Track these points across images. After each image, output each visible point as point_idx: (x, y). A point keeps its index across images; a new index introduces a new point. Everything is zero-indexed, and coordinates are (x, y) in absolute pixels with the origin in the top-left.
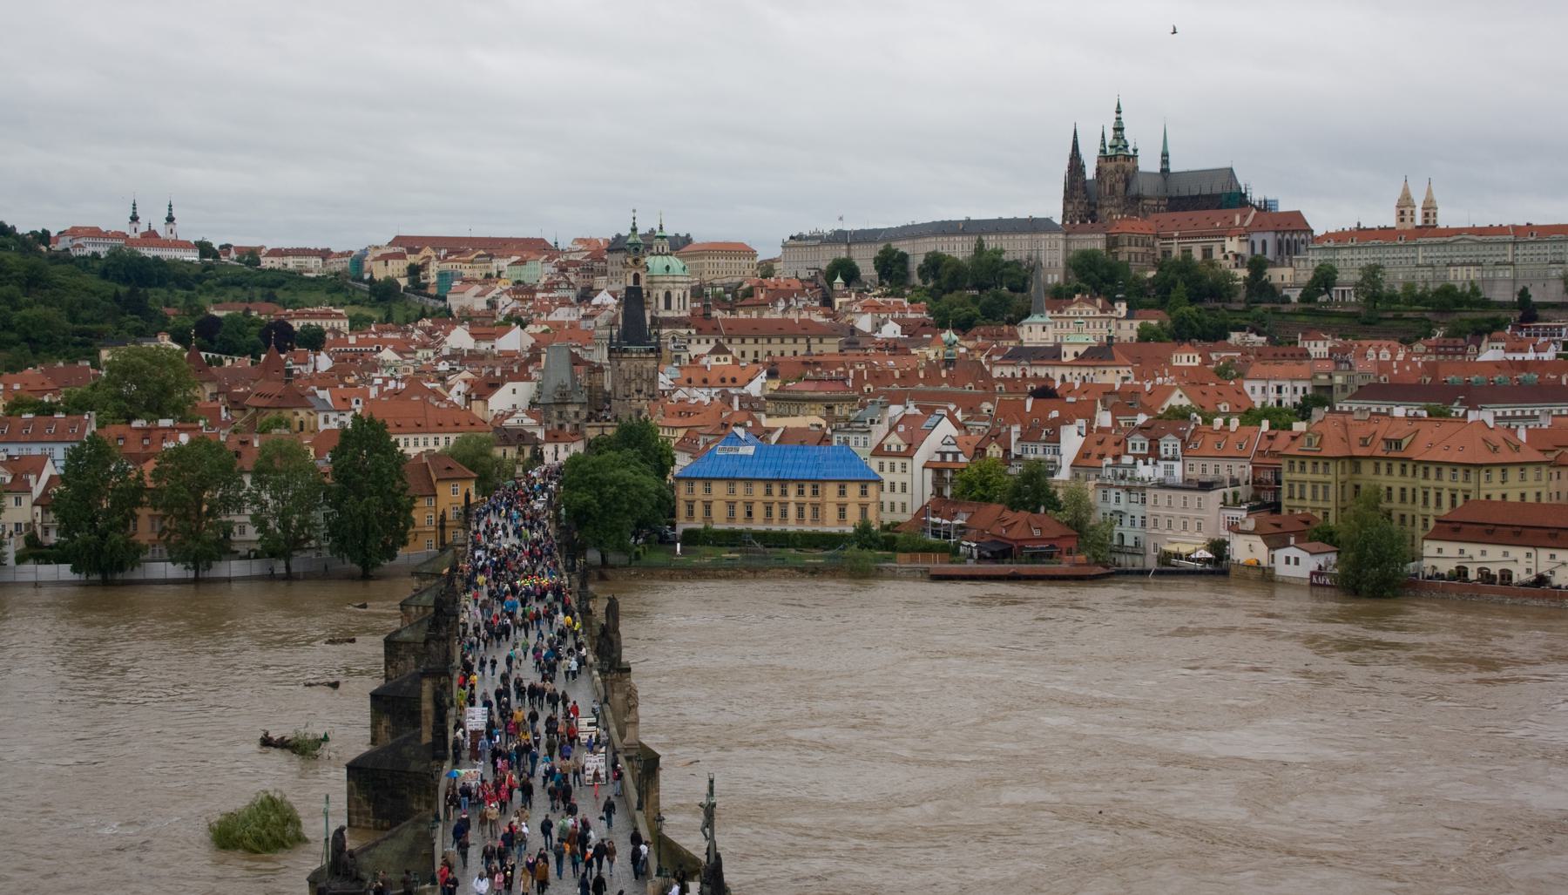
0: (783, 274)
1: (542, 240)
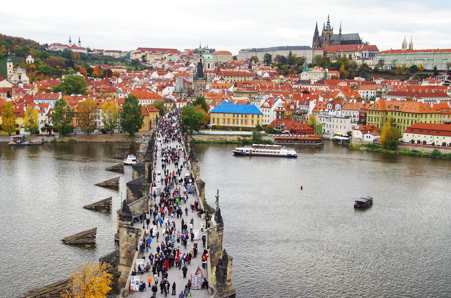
0: (239, 59)
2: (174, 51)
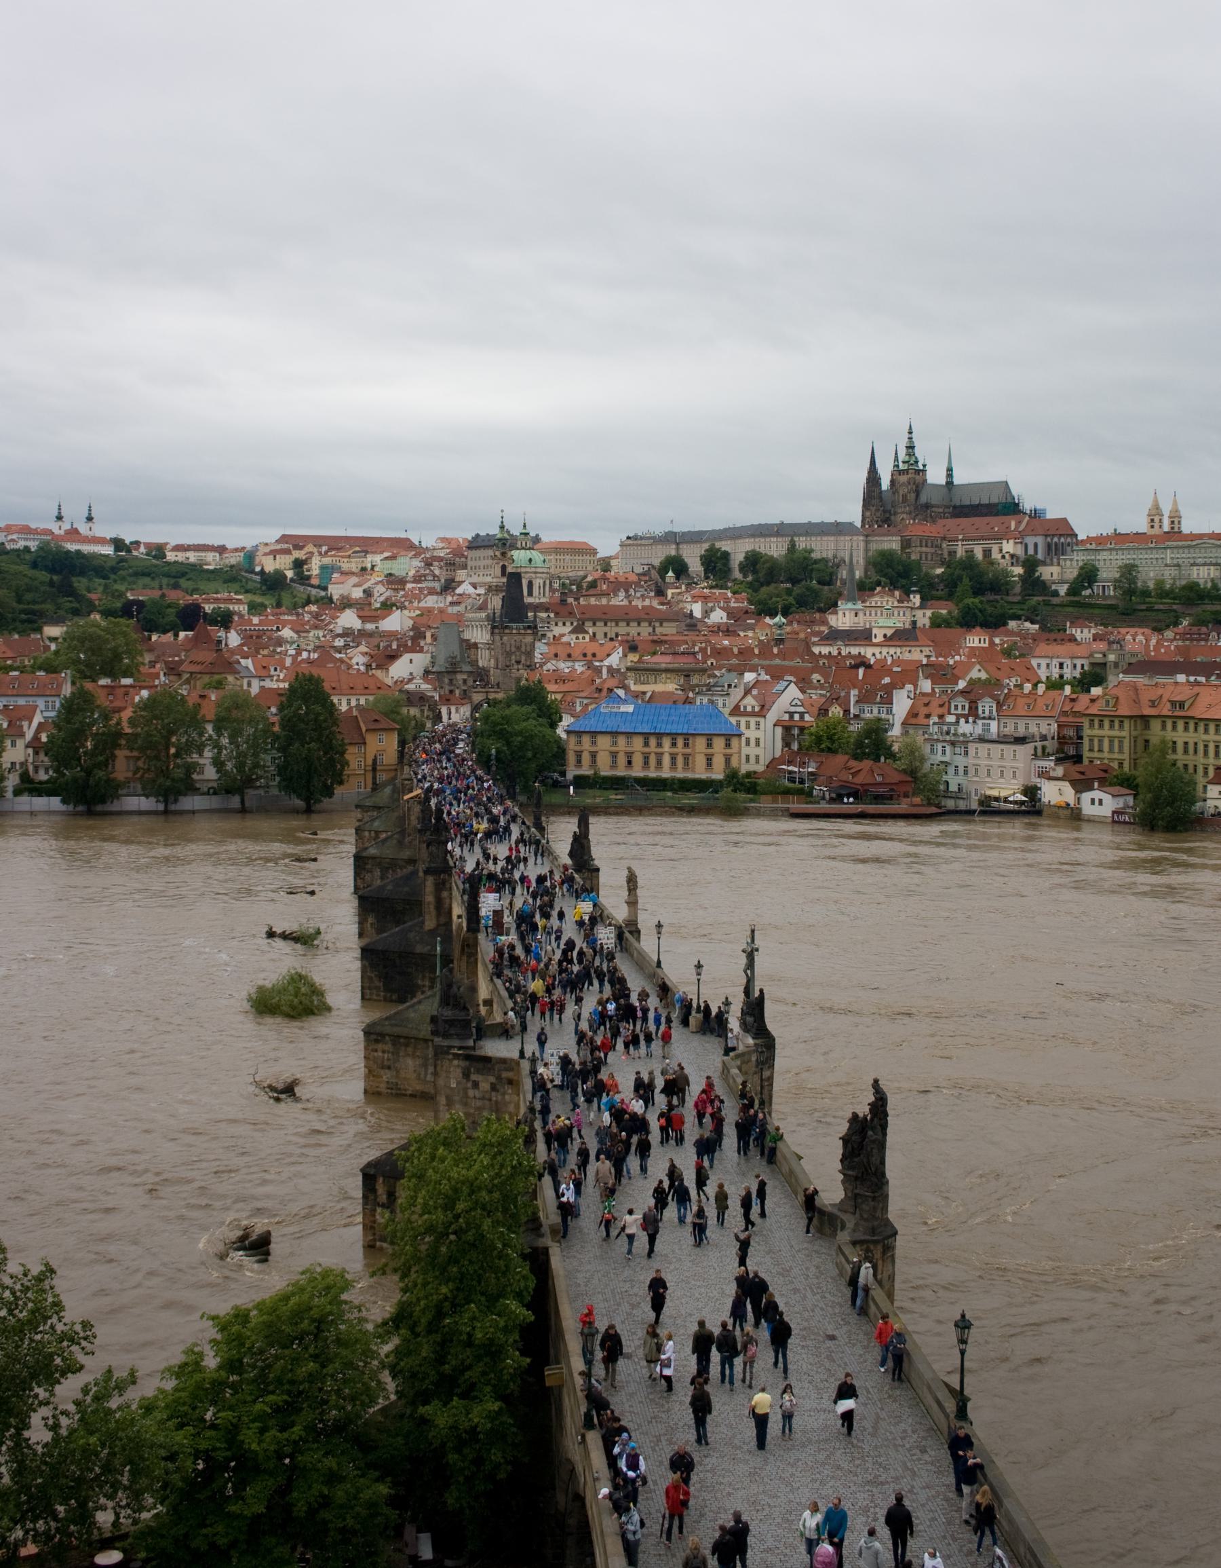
0: (618, 569)
1: (408, 539)
2: (402, 545)
